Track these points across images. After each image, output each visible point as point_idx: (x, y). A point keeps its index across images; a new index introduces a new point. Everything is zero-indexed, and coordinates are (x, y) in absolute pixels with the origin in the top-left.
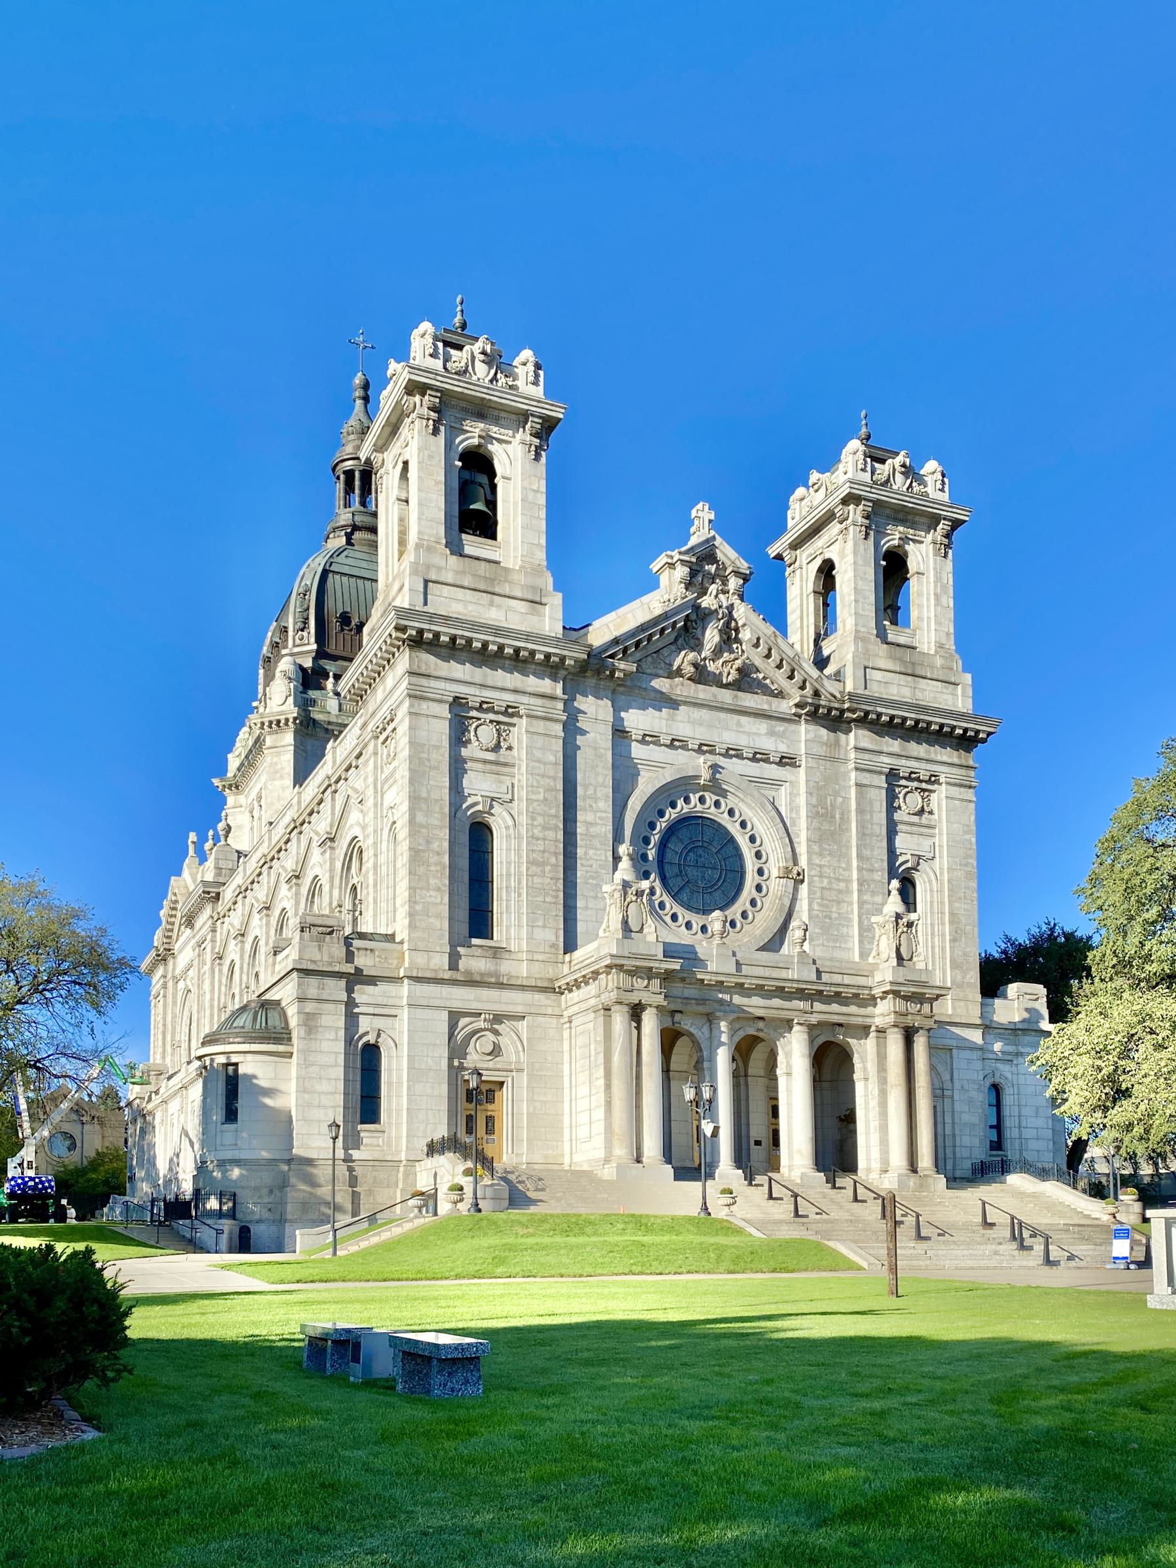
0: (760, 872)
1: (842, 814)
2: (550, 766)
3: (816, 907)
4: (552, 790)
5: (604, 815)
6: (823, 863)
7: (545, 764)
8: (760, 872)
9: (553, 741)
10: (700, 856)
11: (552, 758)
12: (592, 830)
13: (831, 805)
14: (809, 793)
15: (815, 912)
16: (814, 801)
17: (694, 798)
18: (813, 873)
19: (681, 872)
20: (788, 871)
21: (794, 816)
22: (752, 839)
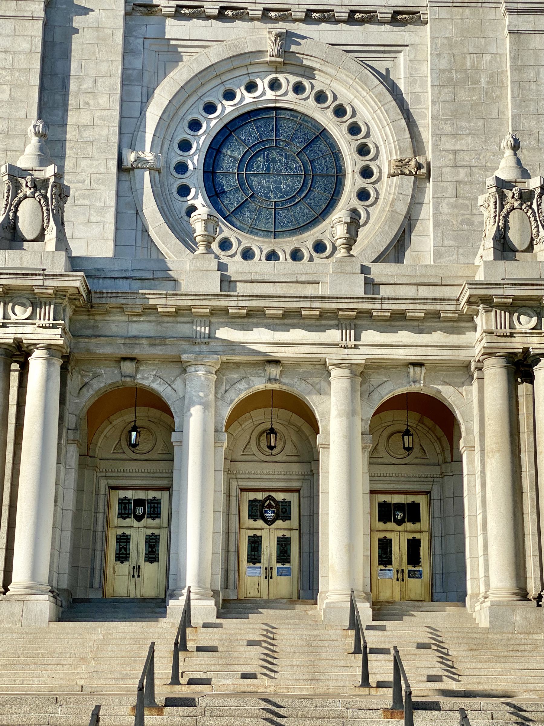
0: (366, 173)
1: (492, 76)
2: (22, 56)
3: (446, 209)
4: (22, 86)
5: (106, 113)
6: (458, 147)
7: (14, 53)
8: (366, 173)
9: (28, 24)
10: (274, 161)
11: (25, 46)
12: (87, 135)
13: (473, 67)
14: (437, 54)
15: (445, 217)
16: (444, 63)
17: (262, 84)
18: (442, 162)
19: (241, 184)
20: (402, 163)
21: (418, 90)
22: (354, 130)
